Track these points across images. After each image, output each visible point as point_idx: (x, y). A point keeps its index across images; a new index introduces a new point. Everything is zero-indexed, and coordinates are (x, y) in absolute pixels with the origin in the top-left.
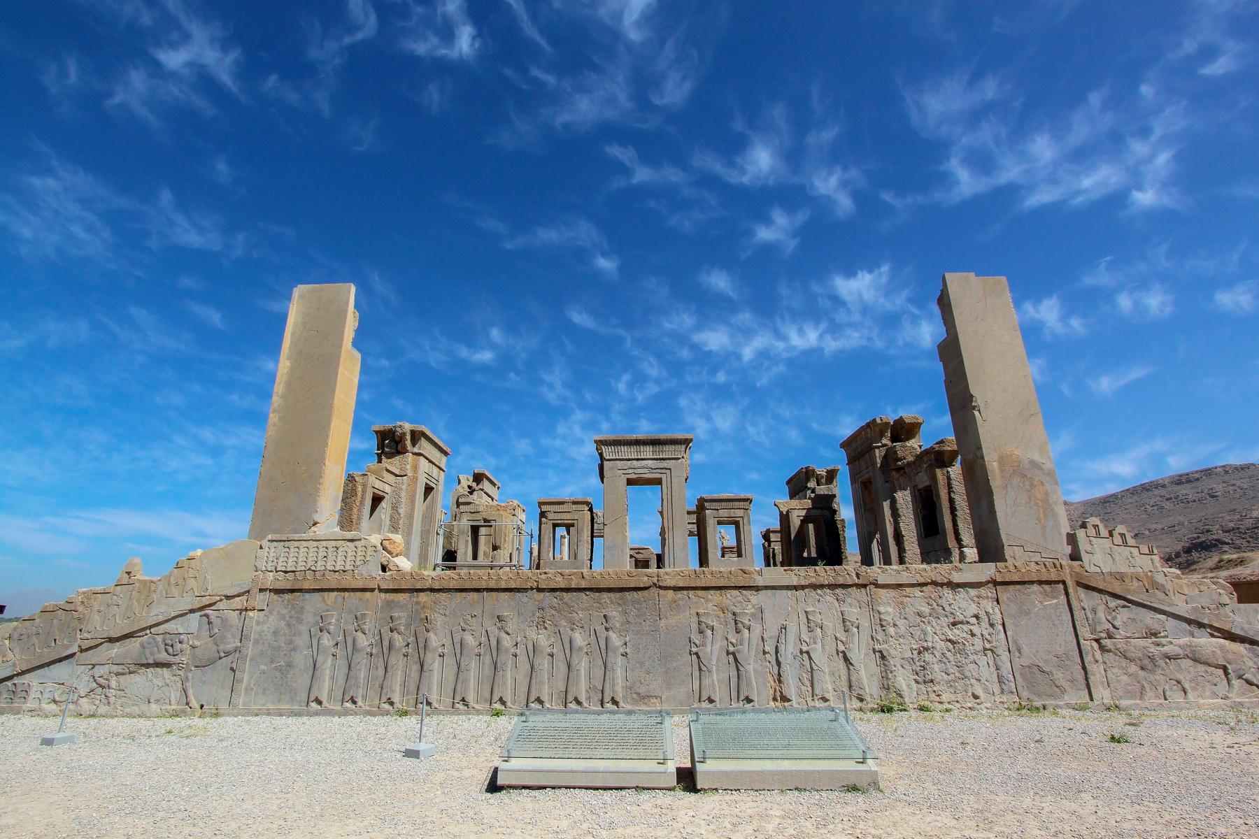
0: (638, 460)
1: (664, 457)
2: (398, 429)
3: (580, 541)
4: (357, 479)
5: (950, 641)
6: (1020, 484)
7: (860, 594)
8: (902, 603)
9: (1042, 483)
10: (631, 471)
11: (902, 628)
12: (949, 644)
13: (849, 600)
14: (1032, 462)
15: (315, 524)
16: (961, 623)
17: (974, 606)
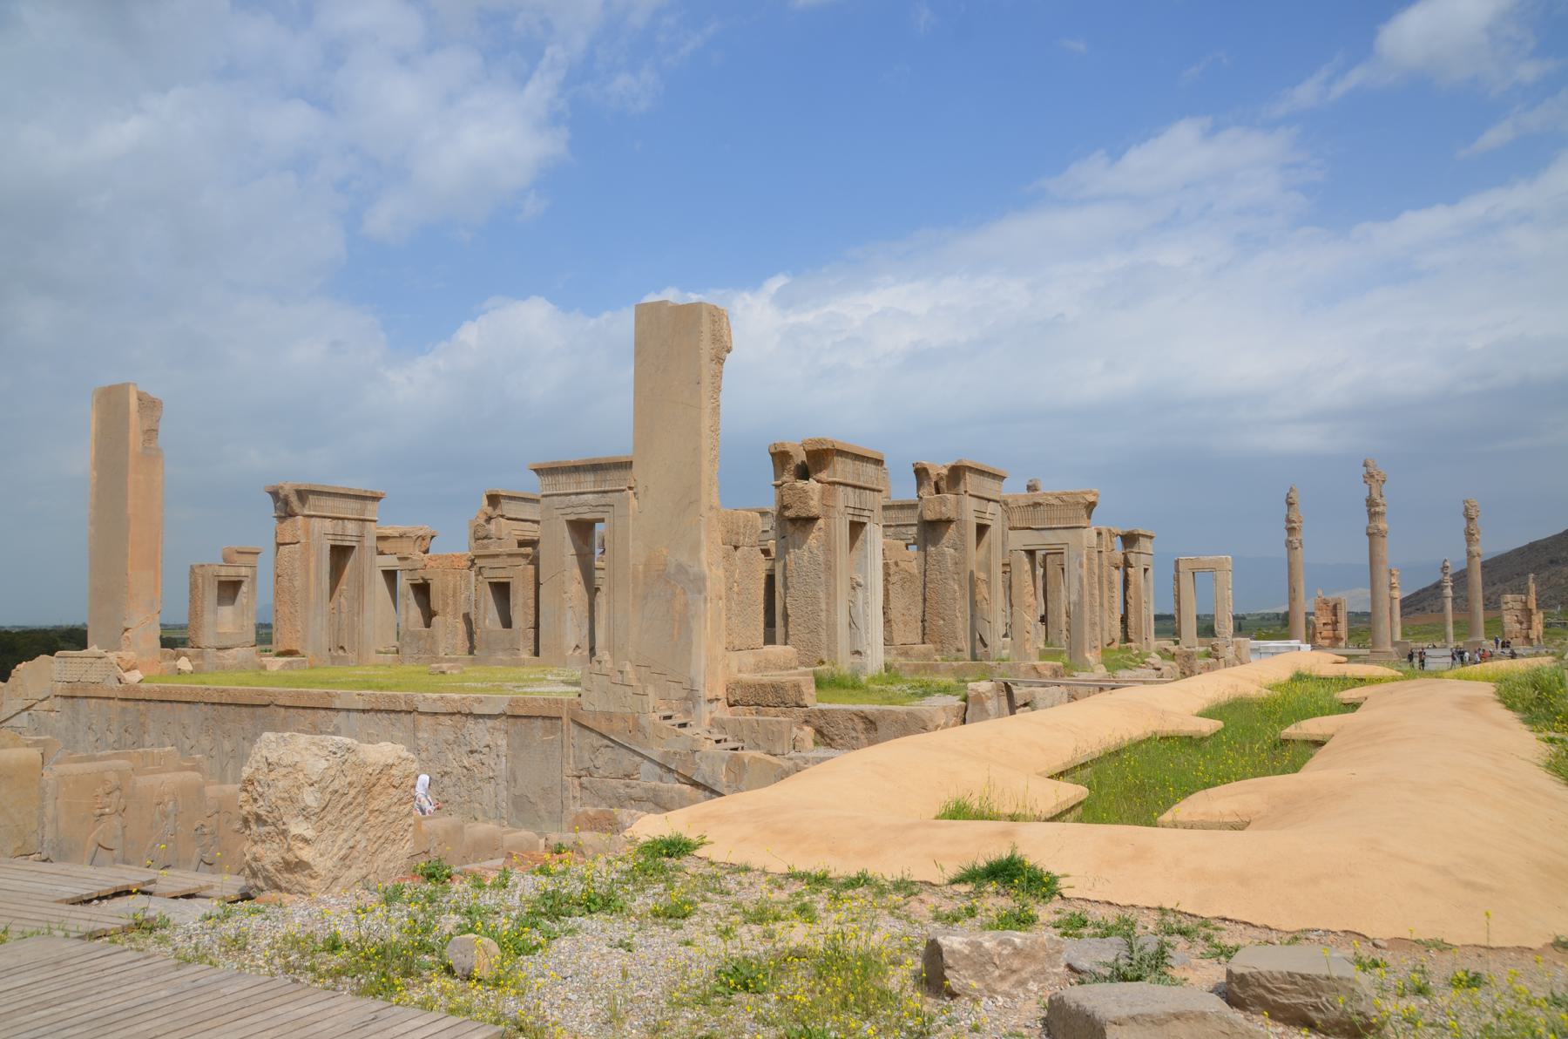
0: (577, 494)
1: (607, 489)
2: (280, 491)
3: (515, 605)
4: (197, 570)
5: (465, 767)
6: (662, 594)
7: (406, 719)
8: (436, 730)
9: (685, 591)
10: (569, 510)
11: (432, 753)
12: (465, 770)
13: (398, 725)
14: (681, 569)
15: (126, 630)
16: (476, 751)
17: (488, 737)
